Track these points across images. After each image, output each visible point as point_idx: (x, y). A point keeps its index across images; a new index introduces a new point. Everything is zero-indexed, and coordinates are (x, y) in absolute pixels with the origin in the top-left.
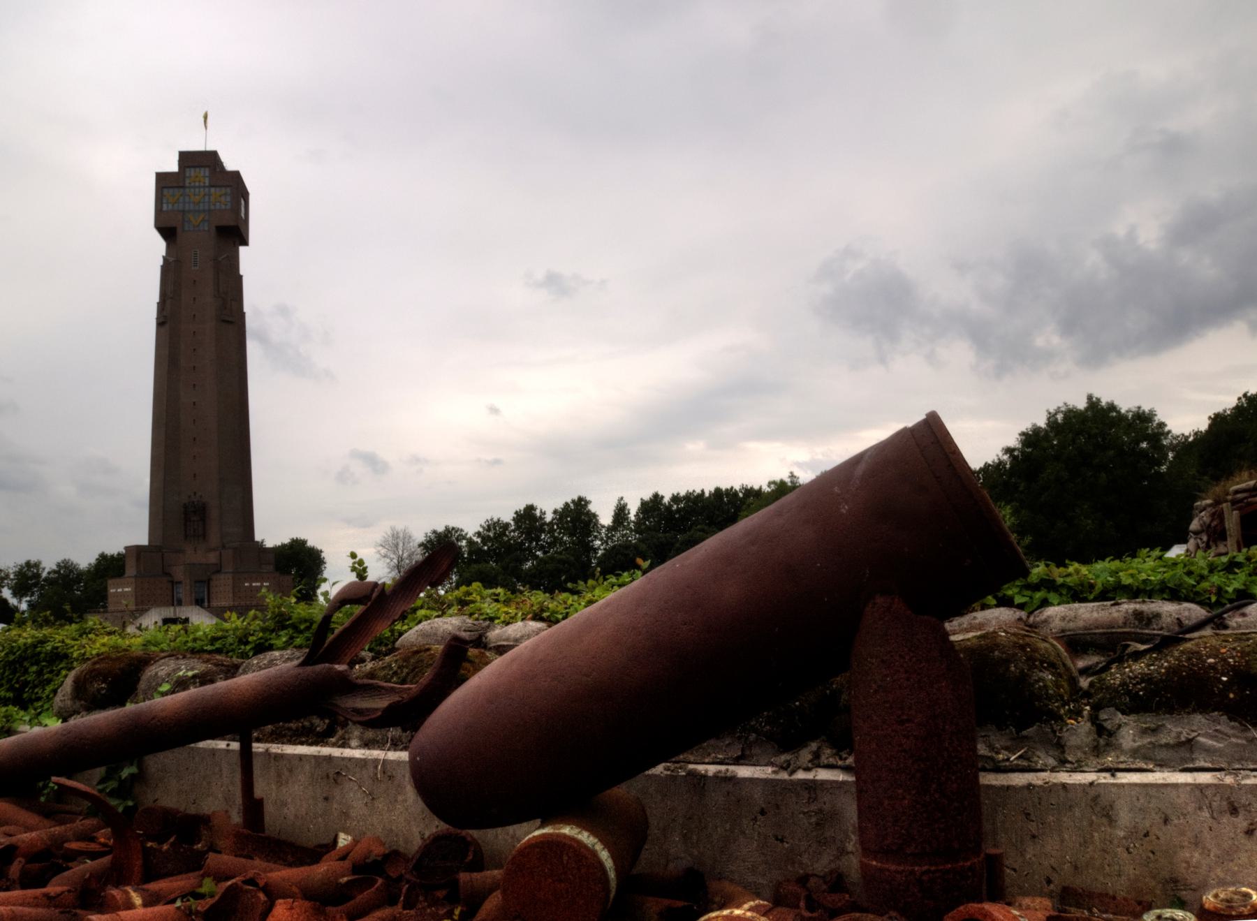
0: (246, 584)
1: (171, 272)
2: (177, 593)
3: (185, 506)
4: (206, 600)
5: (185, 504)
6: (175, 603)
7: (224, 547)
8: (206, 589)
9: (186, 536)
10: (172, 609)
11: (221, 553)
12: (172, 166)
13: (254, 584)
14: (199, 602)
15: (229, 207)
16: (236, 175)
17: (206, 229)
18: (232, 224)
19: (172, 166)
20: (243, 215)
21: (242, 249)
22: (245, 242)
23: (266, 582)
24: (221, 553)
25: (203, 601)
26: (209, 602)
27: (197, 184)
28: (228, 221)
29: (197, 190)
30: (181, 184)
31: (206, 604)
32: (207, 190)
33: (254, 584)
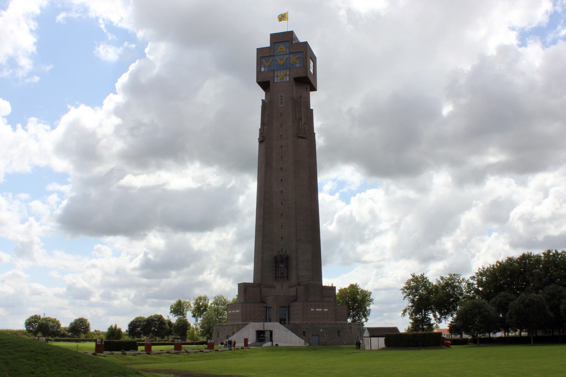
0: (312, 310)
1: (266, 107)
2: (269, 314)
3: (276, 258)
4: (287, 320)
5: (276, 257)
6: (268, 321)
7: (299, 284)
8: (287, 312)
9: (276, 277)
10: (262, 323)
11: (297, 288)
12: (266, 43)
13: (317, 310)
14: (282, 321)
15: (301, 65)
16: (306, 44)
17: (288, 80)
18: (303, 75)
19: (266, 43)
20: (312, 71)
21: (312, 93)
22: (314, 89)
23: (326, 308)
24: (297, 288)
25: (285, 320)
26: (289, 321)
27: (282, 53)
28: (301, 74)
29: (282, 56)
30: (272, 54)
31: (287, 322)
32: (288, 56)
33: (317, 310)
